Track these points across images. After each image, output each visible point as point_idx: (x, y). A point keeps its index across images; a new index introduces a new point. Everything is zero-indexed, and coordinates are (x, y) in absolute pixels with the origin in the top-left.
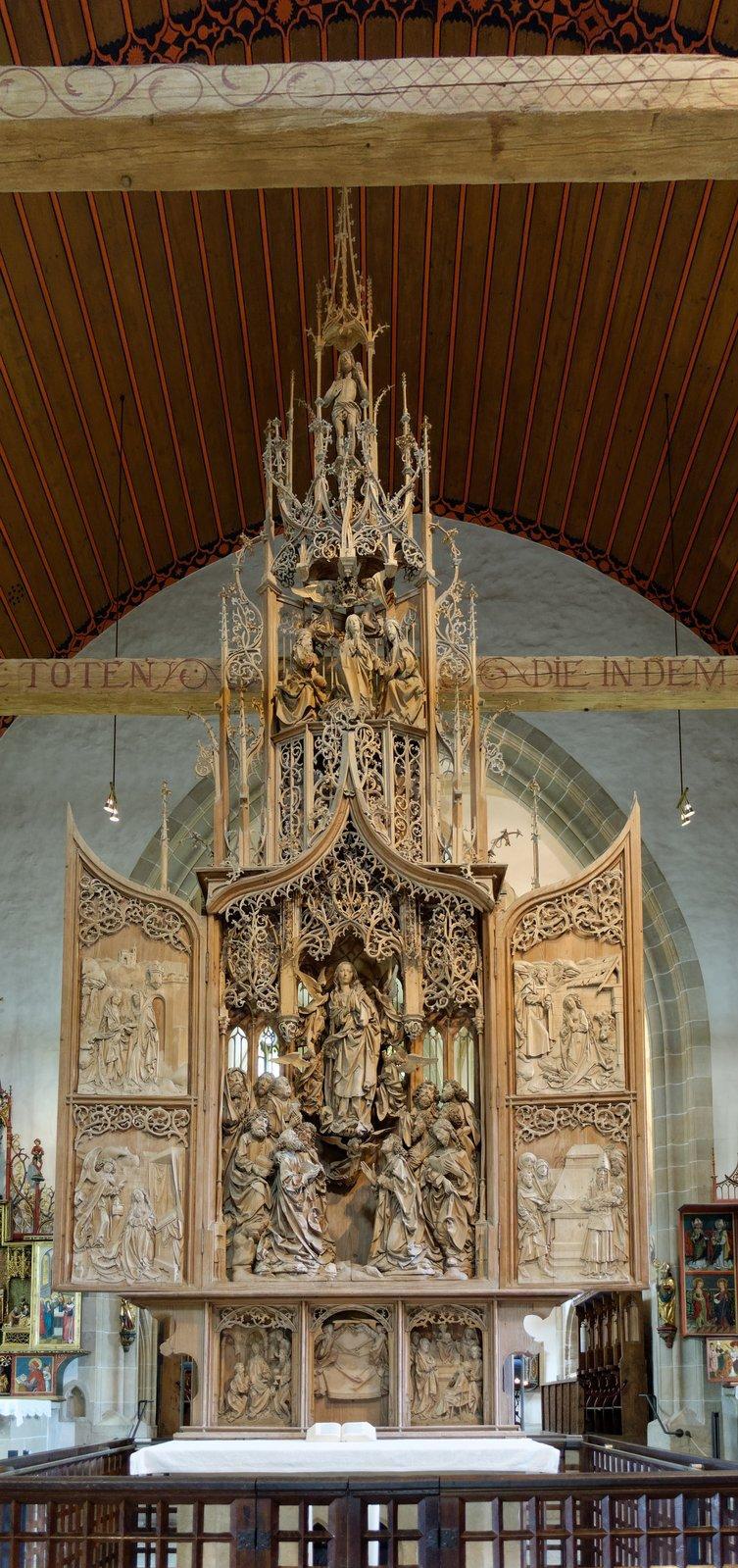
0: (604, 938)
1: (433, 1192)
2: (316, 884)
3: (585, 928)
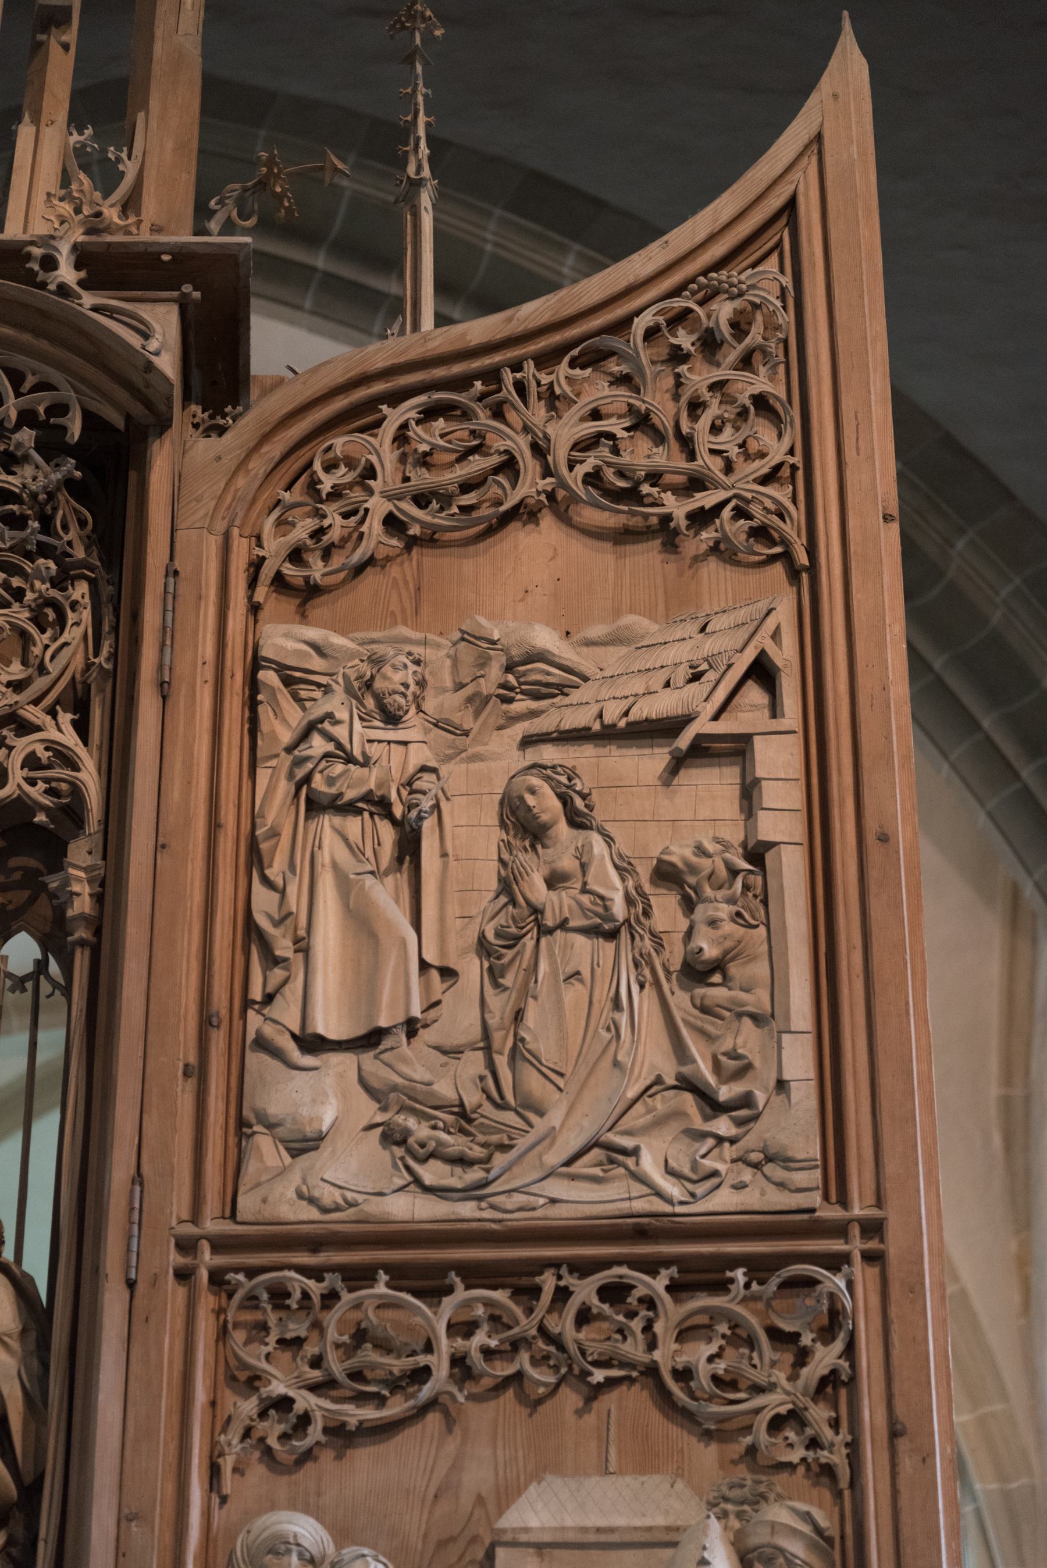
0: (708, 535)
3: (617, 496)
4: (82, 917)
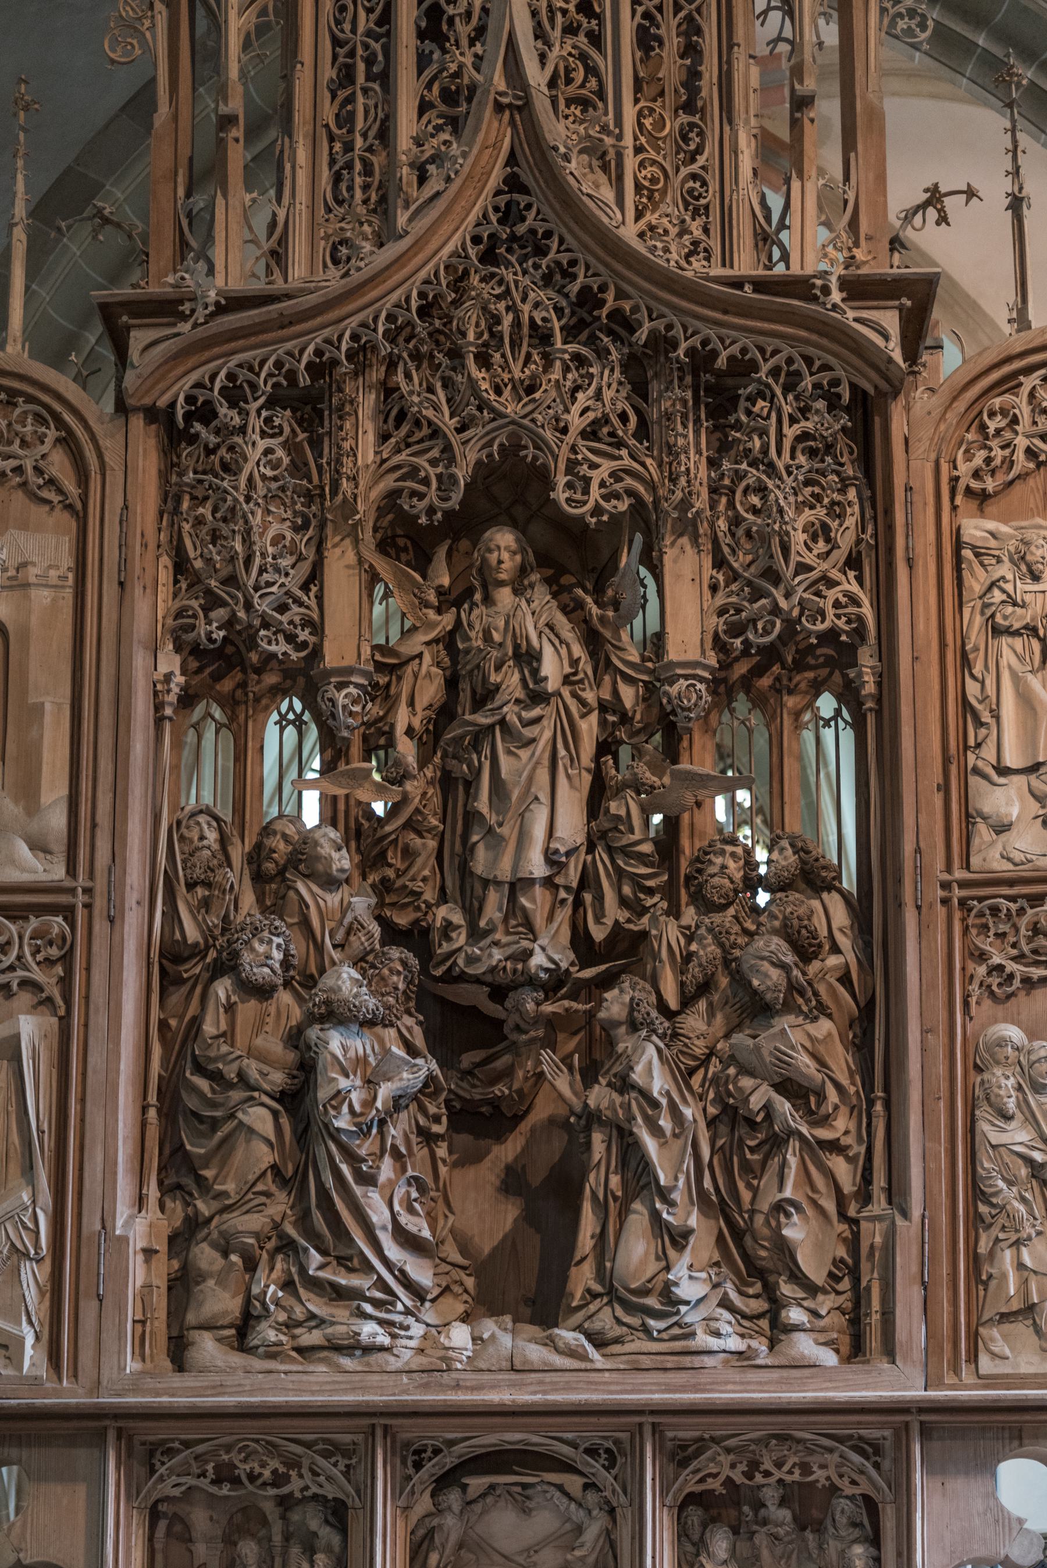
1: (743, 1130)
2: (421, 328)
4: (870, 695)
